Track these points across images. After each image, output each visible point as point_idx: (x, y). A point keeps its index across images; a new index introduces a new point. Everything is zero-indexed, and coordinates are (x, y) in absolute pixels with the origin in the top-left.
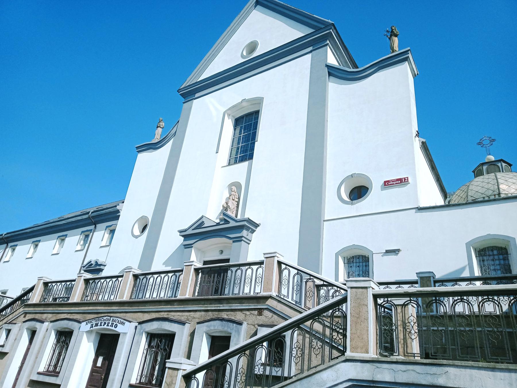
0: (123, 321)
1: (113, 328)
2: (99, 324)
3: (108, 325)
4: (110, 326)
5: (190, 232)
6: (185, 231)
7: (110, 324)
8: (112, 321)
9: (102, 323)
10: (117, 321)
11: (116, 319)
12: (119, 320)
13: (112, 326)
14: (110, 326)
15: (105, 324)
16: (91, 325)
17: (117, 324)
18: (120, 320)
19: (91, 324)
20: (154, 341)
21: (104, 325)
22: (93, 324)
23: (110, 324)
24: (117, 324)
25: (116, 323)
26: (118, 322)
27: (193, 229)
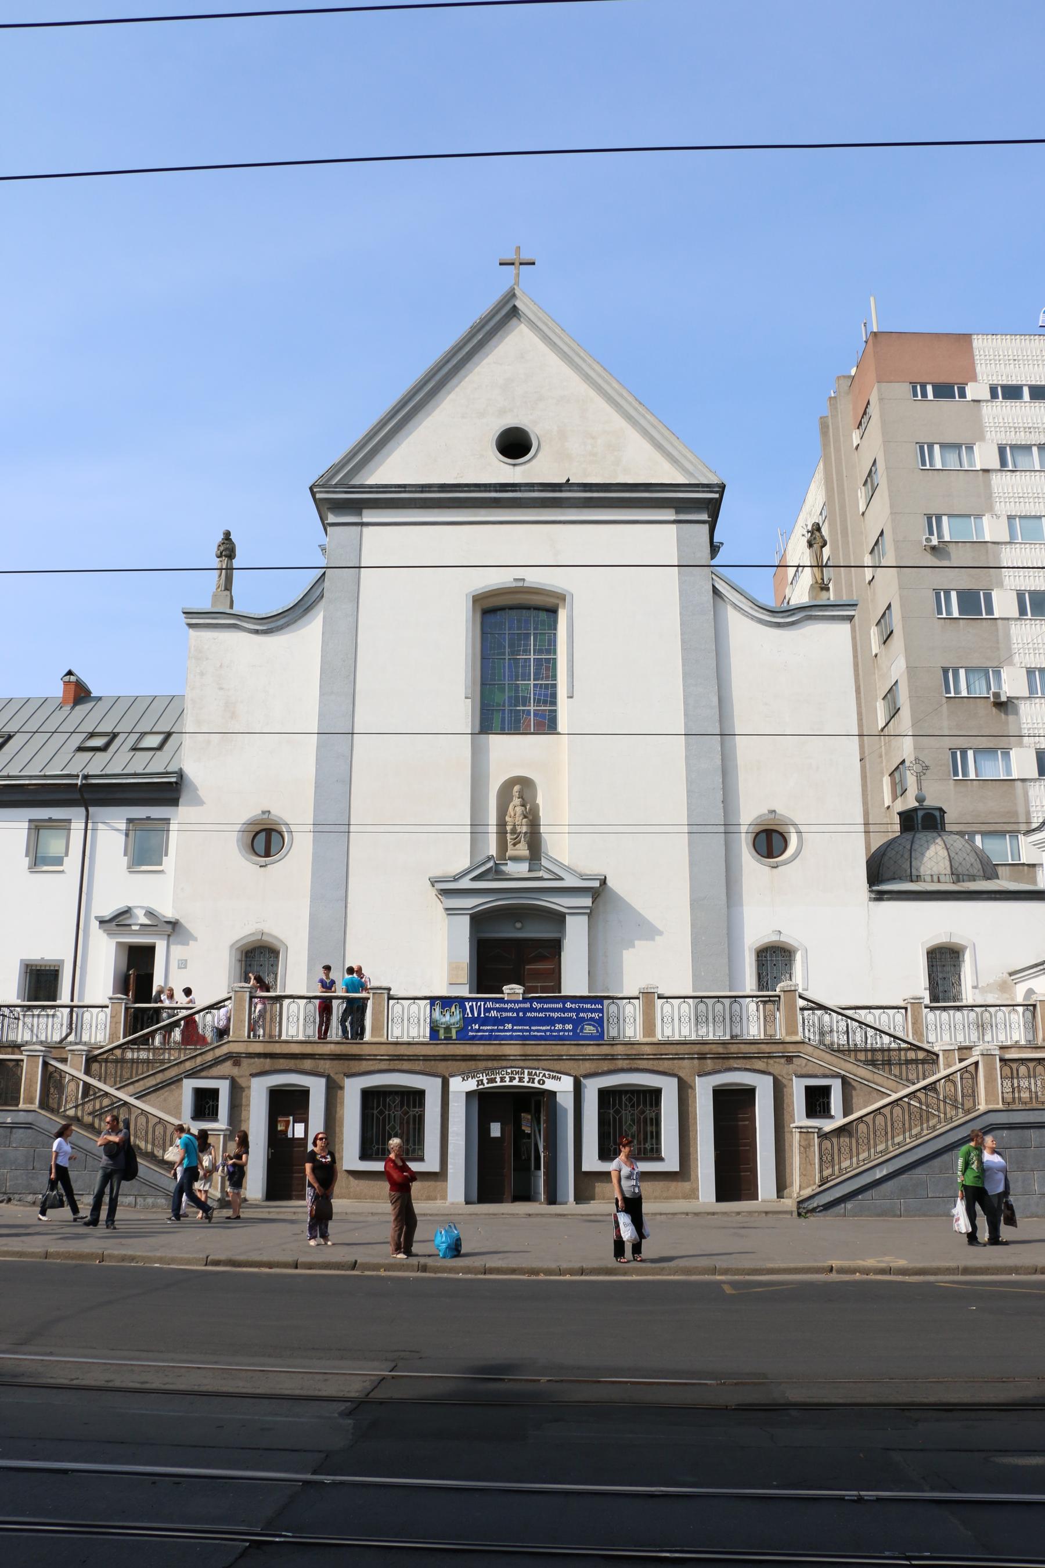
0: (554, 1074)
1: (536, 1085)
2: (498, 1080)
3: (521, 1080)
4: (528, 1082)
5: (465, 883)
6: (456, 879)
7: (526, 1079)
8: (529, 1074)
9: (505, 1077)
10: (541, 1075)
11: (538, 1072)
12: (545, 1074)
13: (533, 1082)
14: (528, 1082)
15: (512, 1079)
16: (478, 1081)
17: (544, 1078)
18: (547, 1073)
19: (477, 1079)
20: (555, 1093)
21: (511, 1081)
22: (482, 1080)
23: (526, 1079)
24: (544, 1078)
25: (540, 1078)
26: (544, 1075)
27: (473, 879)
